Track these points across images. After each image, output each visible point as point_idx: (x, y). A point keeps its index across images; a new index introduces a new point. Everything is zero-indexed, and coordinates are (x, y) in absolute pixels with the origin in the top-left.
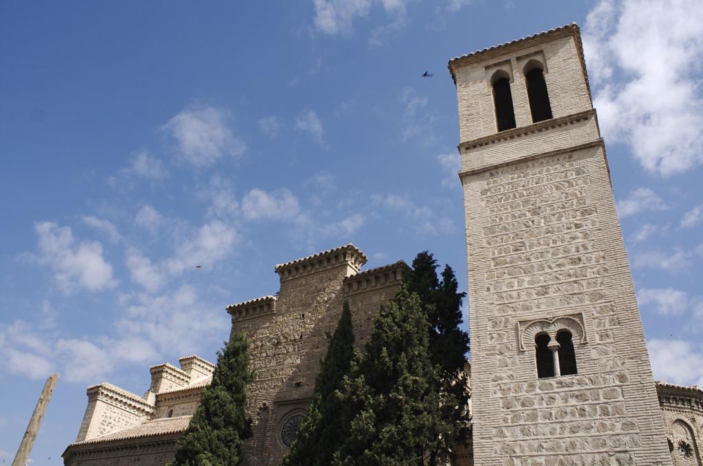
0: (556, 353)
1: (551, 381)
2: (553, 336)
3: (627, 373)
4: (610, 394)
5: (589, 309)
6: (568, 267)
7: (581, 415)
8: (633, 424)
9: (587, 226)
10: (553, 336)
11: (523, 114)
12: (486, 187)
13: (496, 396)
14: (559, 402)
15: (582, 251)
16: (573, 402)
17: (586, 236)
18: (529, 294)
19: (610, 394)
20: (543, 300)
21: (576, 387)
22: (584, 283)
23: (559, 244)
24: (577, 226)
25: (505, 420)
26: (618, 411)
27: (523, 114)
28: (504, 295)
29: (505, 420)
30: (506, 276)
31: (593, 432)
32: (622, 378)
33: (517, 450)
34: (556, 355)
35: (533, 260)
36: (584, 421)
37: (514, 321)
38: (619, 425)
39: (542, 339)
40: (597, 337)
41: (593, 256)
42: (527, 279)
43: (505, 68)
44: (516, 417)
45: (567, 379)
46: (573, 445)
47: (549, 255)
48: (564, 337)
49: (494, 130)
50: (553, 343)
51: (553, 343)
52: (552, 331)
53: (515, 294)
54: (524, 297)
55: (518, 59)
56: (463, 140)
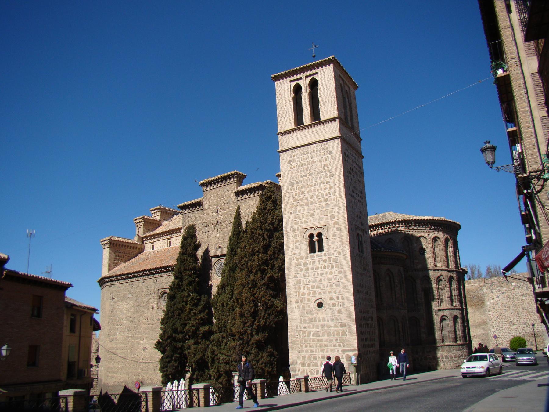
0: (316, 243)
1: (314, 254)
2: (315, 235)
3: (341, 251)
4: (335, 260)
5: (331, 223)
6: (323, 203)
7: (325, 268)
8: (341, 271)
9: (331, 183)
10: (315, 235)
11: (307, 118)
12: (290, 159)
13: (293, 261)
14: (317, 263)
15: (328, 195)
16: (322, 262)
17: (331, 188)
18: (307, 216)
19: (335, 260)
20: (312, 219)
21: (323, 257)
22: (328, 211)
23: (320, 191)
24: (328, 182)
25: (297, 271)
26: (337, 266)
27: (307, 118)
28: (297, 216)
29: (297, 271)
30: (299, 207)
31: (328, 275)
32: (339, 253)
33: (302, 283)
34: (316, 243)
35: (309, 199)
36: (324, 271)
37: (301, 228)
38: (337, 272)
39: (311, 236)
40: (332, 235)
41: (333, 198)
42: (306, 209)
43: (300, 82)
44: (301, 270)
45: (320, 253)
46: (321, 280)
47: (315, 197)
48: (320, 235)
49: (293, 126)
50: (315, 238)
51: (315, 238)
52: (315, 233)
53: (301, 216)
54: (305, 217)
55: (306, 77)
56: (279, 132)
